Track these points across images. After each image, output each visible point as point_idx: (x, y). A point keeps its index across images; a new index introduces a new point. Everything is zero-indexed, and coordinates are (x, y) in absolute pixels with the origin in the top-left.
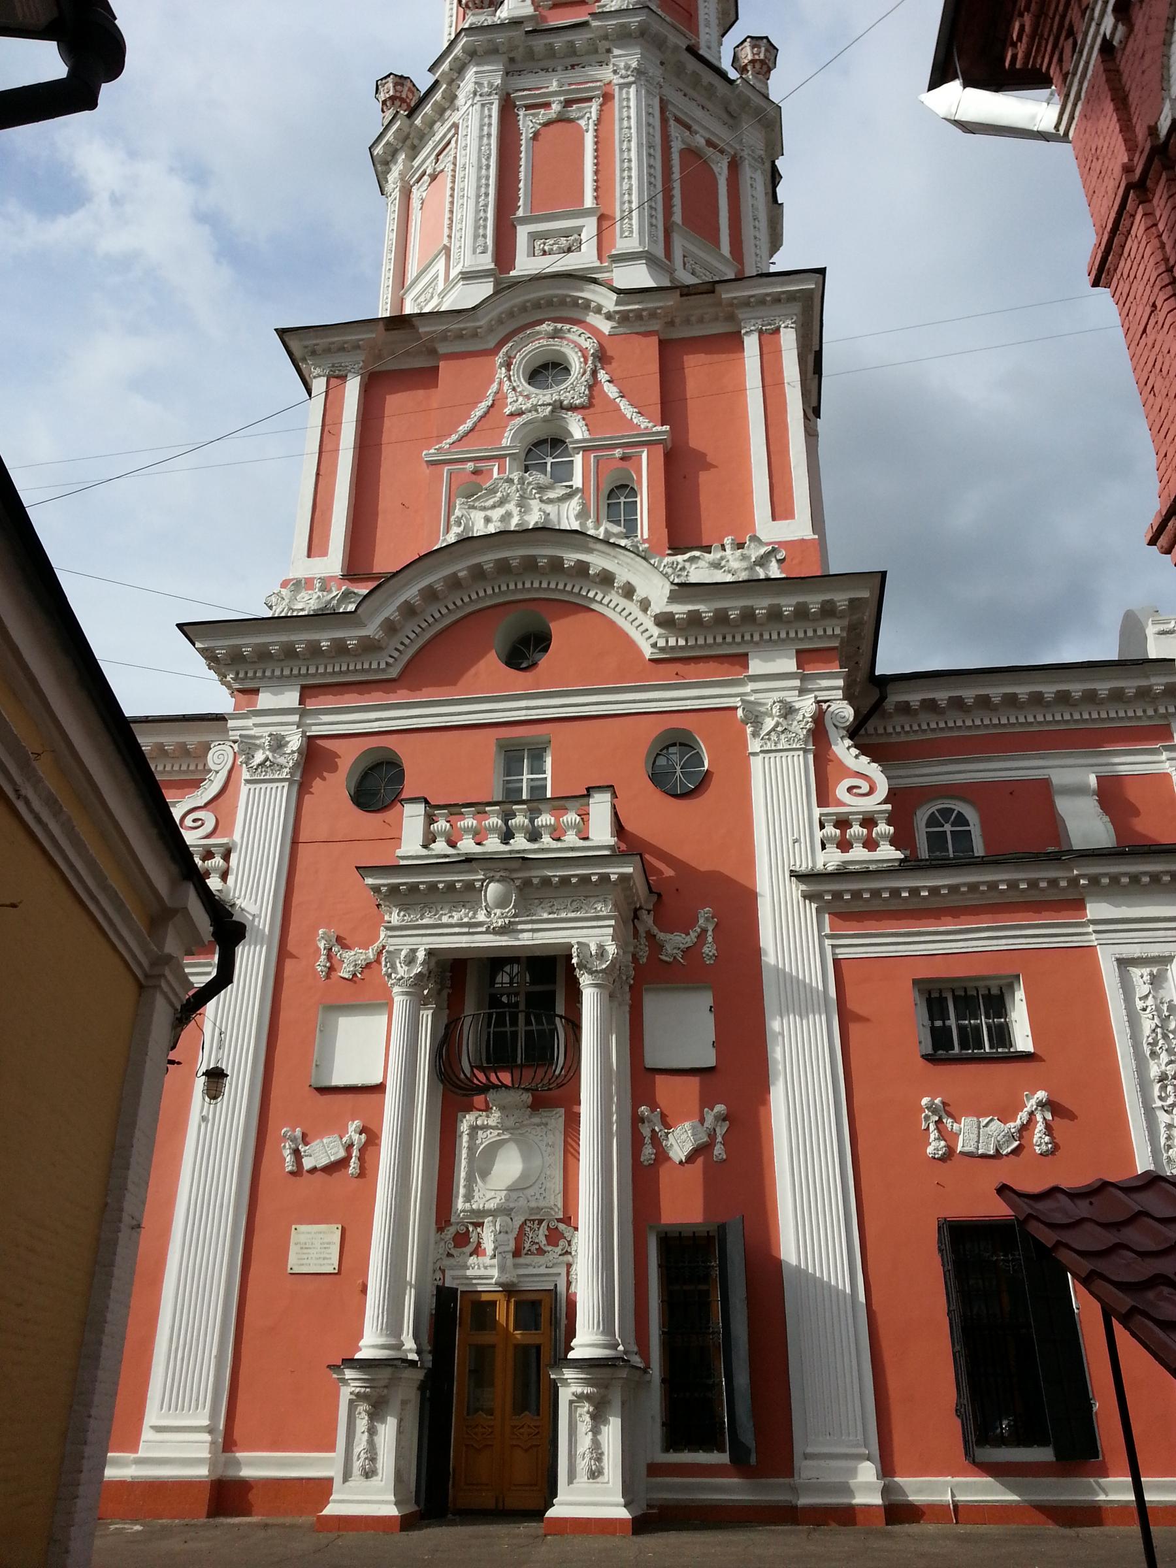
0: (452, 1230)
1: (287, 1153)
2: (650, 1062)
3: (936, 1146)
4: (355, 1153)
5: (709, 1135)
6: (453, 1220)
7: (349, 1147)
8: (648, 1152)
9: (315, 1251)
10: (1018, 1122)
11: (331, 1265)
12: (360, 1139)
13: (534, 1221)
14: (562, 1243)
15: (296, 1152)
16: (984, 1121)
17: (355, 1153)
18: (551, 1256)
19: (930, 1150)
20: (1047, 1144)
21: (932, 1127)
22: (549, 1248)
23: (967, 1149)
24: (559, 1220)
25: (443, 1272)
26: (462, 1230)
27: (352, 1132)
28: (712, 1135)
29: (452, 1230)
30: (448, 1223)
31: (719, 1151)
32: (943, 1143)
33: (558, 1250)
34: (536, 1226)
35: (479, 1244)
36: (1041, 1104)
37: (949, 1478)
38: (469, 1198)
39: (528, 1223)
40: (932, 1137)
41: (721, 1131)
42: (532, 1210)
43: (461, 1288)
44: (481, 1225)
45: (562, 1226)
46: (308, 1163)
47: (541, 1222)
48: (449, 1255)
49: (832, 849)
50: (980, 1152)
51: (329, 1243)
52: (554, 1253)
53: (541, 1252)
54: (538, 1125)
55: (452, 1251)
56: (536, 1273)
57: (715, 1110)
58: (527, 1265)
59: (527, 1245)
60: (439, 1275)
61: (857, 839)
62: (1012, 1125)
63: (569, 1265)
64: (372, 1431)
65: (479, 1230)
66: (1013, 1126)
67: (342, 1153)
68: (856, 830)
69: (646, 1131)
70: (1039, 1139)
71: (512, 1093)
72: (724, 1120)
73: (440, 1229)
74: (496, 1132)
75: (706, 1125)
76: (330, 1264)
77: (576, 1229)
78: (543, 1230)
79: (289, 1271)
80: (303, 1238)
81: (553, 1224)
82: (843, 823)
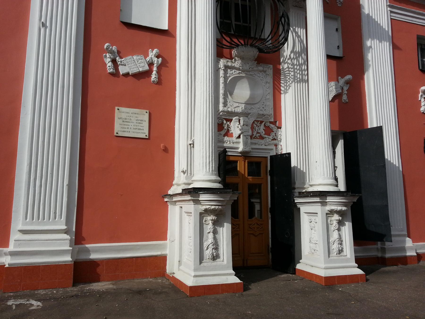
1: (108, 61)
4: (155, 69)
7: (151, 64)
9: (132, 124)
12: (158, 61)
13: (258, 121)
15: (114, 61)
17: (155, 69)
22: (266, 136)
24: (271, 123)
27: (152, 54)
31: (345, 97)
33: (271, 137)
34: (259, 124)
35: (228, 131)
38: (225, 104)
41: (346, 88)
42: (260, 115)
44: (231, 120)
45: (272, 126)
46: (122, 70)
47: (261, 122)
51: (142, 120)
52: (268, 139)
53: (262, 138)
58: (256, 144)
63: (276, 145)
64: (215, 232)
65: (228, 123)
67: (147, 68)
72: (347, 84)
74: (238, 72)
78: (262, 127)
79: (115, 134)
80: (124, 116)
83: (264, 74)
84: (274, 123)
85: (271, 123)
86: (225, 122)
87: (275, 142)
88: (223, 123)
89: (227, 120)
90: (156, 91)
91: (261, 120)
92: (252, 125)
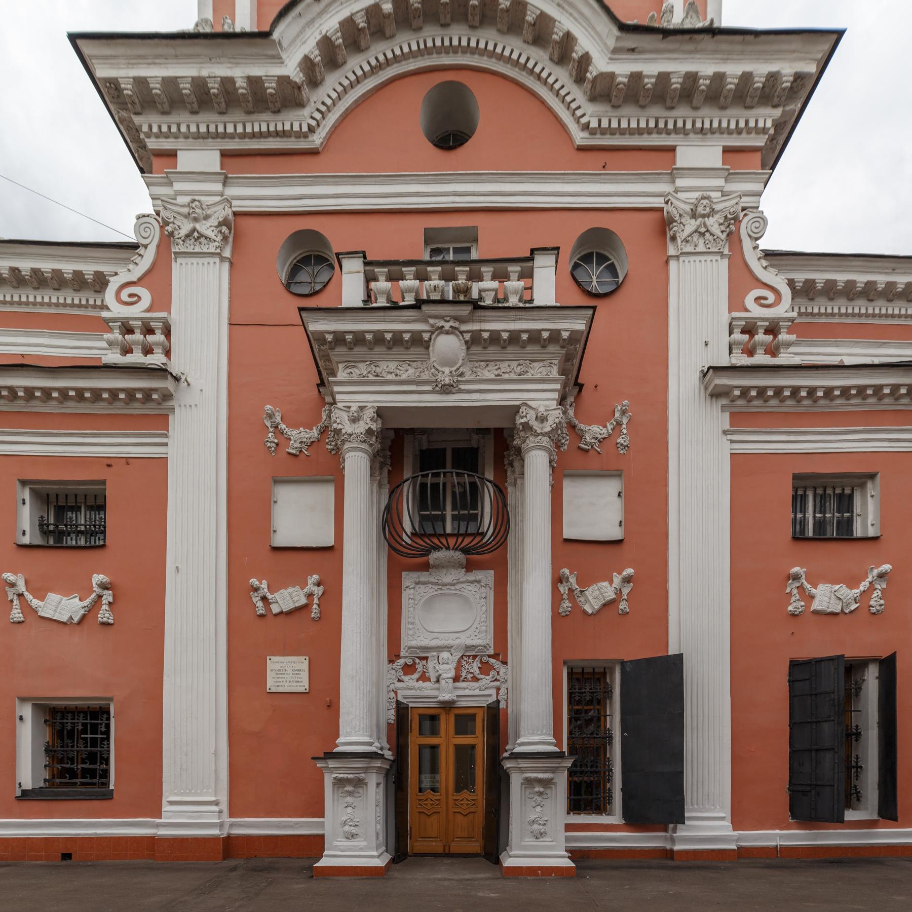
0: (401, 662)
2: (568, 533)
3: (797, 605)
5: (616, 594)
6: (402, 654)
8: (566, 604)
10: (862, 588)
11: (302, 684)
13: (469, 656)
14: (492, 673)
16: (837, 587)
18: (484, 682)
19: (790, 608)
20: (881, 605)
21: (795, 591)
22: (482, 676)
23: (819, 608)
24: (490, 656)
25: (396, 693)
26: (409, 662)
28: (619, 592)
29: (401, 662)
30: (398, 657)
31: (623, 605)
32: (803, 603)
34: (471, 660)
36: (881, 576)
37: (778, 831)
39: (465, 658)
40: (793, 599)
41: (626, 591)
42: (468, 648)
43: (411, 705)
44: (426, 658)
45: (492, 661)
47: (475, 657)
48: (399, 681)
49: (737, 351)
50: (829, 610)
52: (486, 680)
53: (475, 679)
54: (472, 582)
55: (403, 678)
56: (475, 694)
57: (624, 573)
59: (464, 674)
60: (392, 695)
61: (762, 344)
62: (857, 591)
66: (856, 592)
68: (760, 337)
69: (563, 589)
70: (875, 601)
71: (452, 553)
72: (629, 582)
73: (391, 661)
74: (436, 587)
75: (614, 585)
76: (302, 684)
77: (505, 663)
78: (476, 665)
81: (485, 659)
82: (749, 330)
83: (479, 586)
84: (495, 656)
85: (490, 656)
86: (417, 661)
87: (497, 683)
88: (414, 663)
89: (421, 659)
90: (316, 631)
91: (473, 653)
92: (459, 662)
